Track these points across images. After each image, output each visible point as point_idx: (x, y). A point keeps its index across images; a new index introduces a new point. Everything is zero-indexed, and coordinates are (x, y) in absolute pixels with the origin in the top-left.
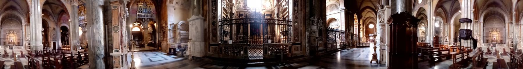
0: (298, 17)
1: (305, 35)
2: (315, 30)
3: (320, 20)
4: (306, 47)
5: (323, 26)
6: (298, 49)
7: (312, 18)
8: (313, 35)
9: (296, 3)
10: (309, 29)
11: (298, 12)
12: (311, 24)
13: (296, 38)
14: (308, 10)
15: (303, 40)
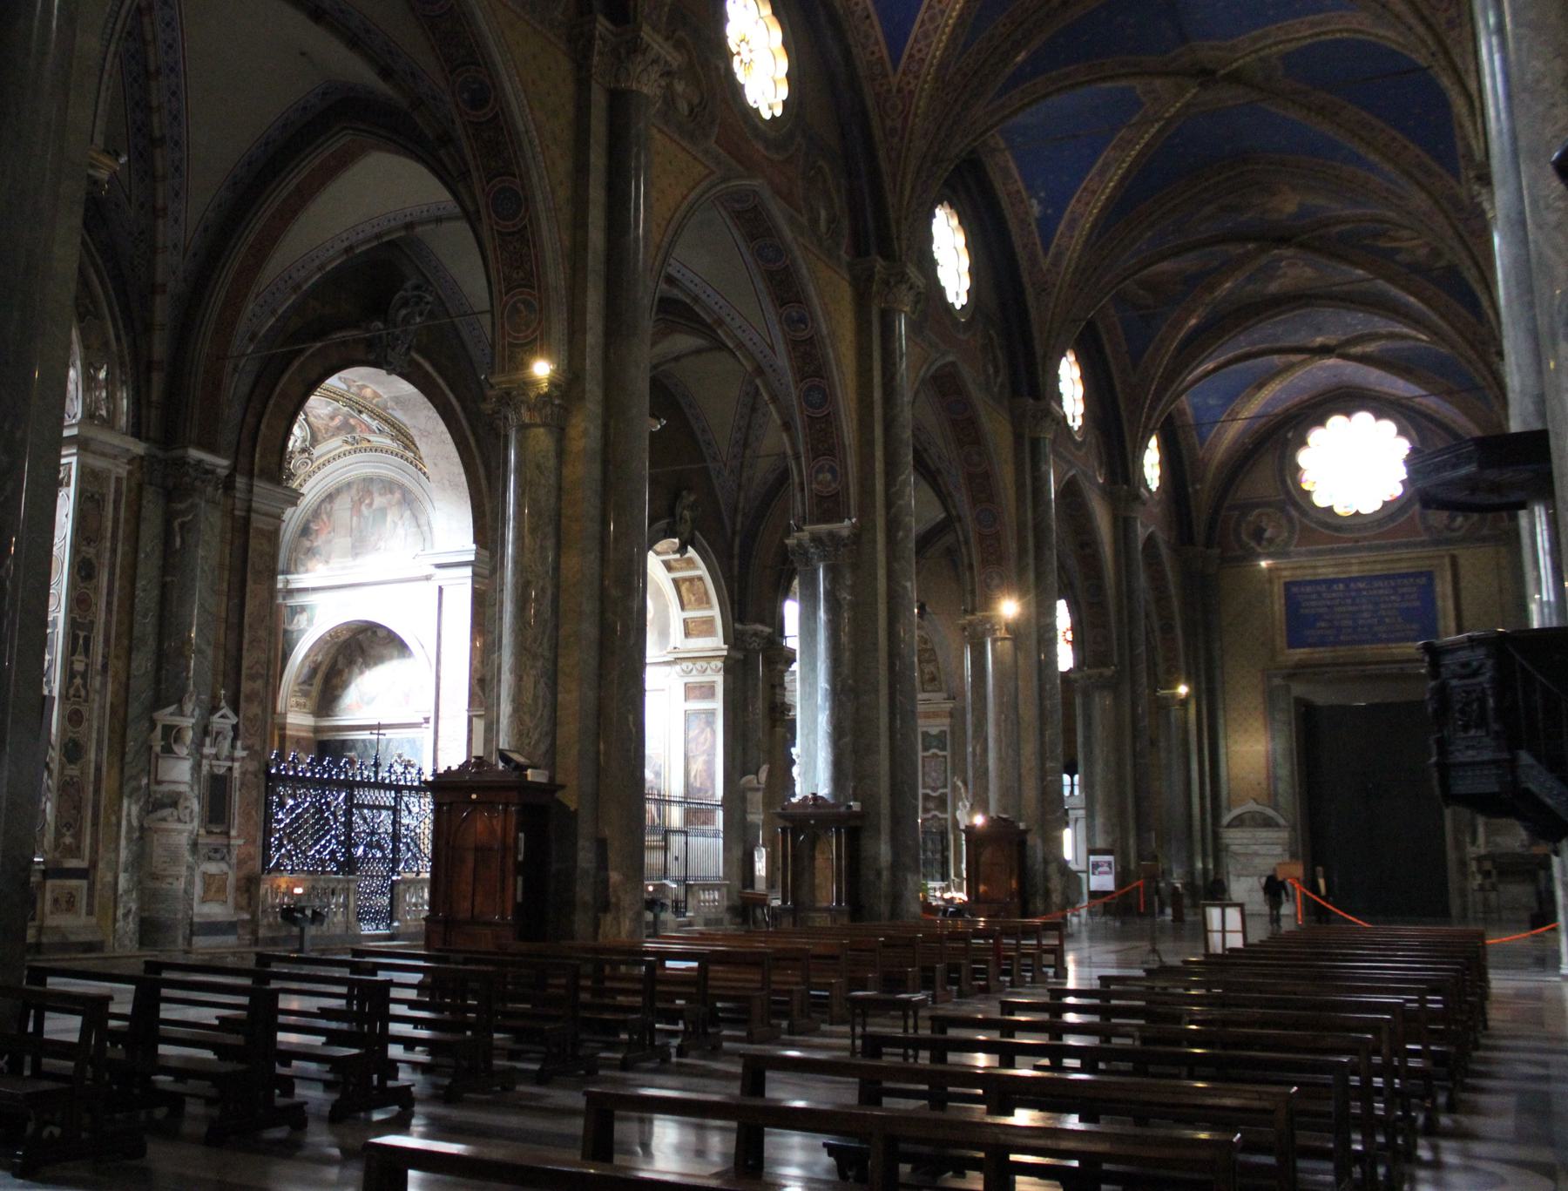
0: (86, 715)
1: (114, 819)
2: (184, 788)
3: (215, 718)
4: (120, 891)
5: (240, 753)
6: (70, 904)
7: (165, 716)
8: (164, 819)
9: (82, 634)
10: (144, 781)
11: (85, 685)
12: (158, 749)
13: (68, 840)
14: (143, 662)
15: (101, 850)
